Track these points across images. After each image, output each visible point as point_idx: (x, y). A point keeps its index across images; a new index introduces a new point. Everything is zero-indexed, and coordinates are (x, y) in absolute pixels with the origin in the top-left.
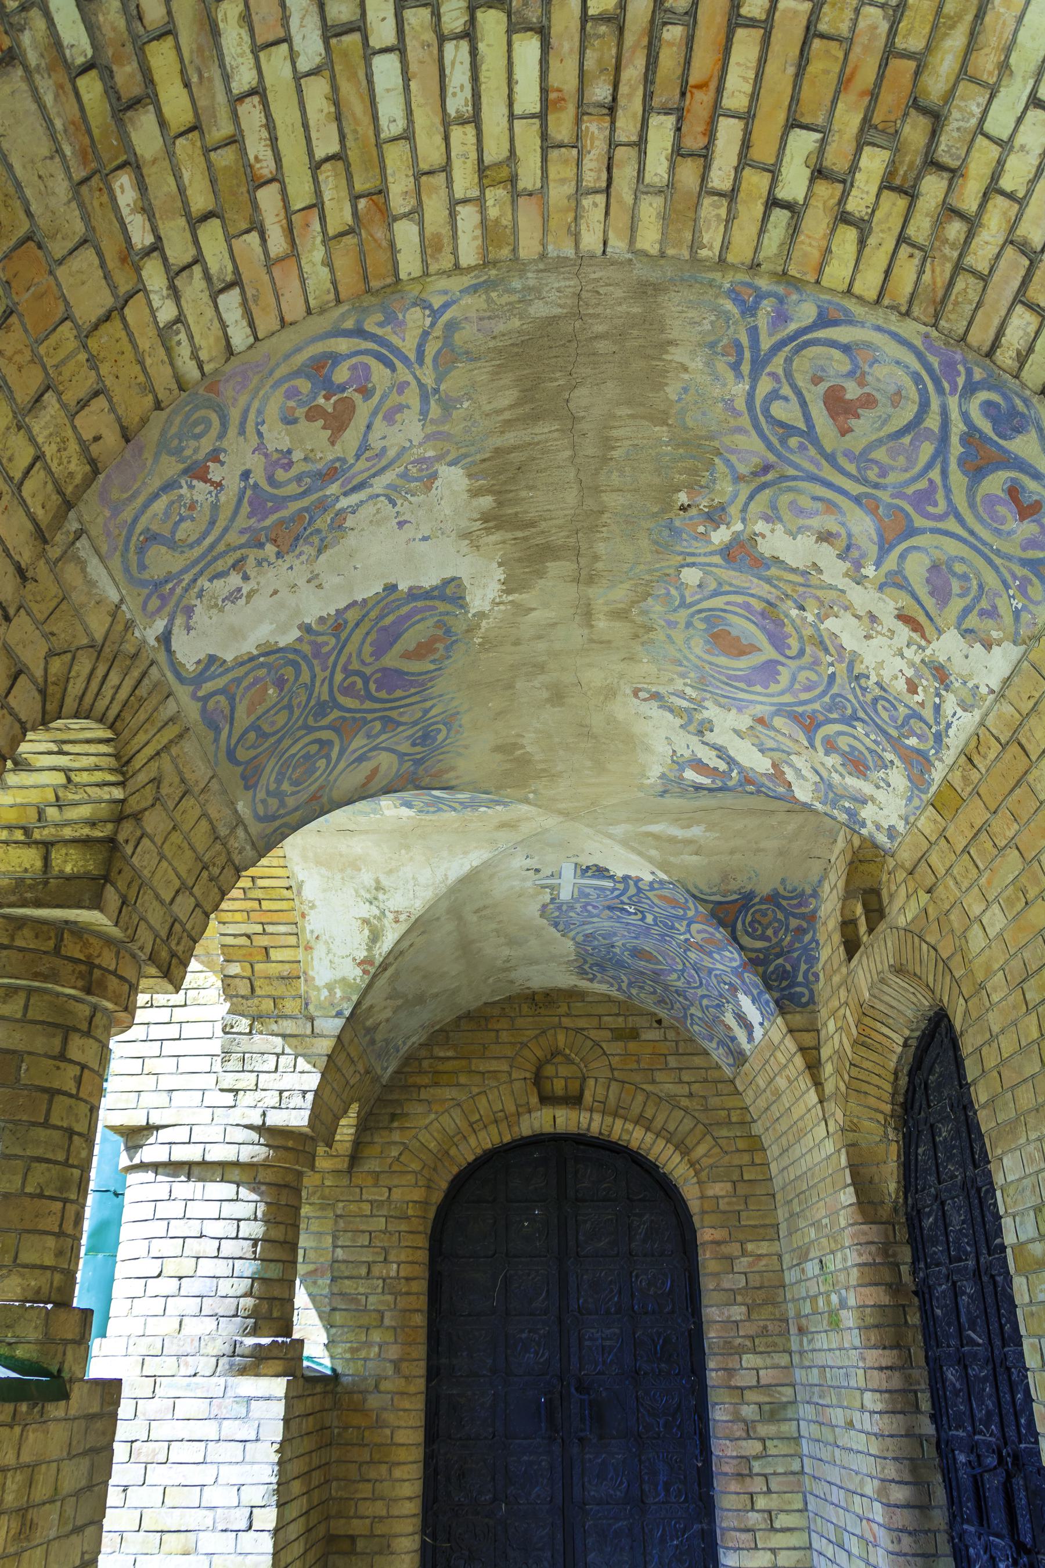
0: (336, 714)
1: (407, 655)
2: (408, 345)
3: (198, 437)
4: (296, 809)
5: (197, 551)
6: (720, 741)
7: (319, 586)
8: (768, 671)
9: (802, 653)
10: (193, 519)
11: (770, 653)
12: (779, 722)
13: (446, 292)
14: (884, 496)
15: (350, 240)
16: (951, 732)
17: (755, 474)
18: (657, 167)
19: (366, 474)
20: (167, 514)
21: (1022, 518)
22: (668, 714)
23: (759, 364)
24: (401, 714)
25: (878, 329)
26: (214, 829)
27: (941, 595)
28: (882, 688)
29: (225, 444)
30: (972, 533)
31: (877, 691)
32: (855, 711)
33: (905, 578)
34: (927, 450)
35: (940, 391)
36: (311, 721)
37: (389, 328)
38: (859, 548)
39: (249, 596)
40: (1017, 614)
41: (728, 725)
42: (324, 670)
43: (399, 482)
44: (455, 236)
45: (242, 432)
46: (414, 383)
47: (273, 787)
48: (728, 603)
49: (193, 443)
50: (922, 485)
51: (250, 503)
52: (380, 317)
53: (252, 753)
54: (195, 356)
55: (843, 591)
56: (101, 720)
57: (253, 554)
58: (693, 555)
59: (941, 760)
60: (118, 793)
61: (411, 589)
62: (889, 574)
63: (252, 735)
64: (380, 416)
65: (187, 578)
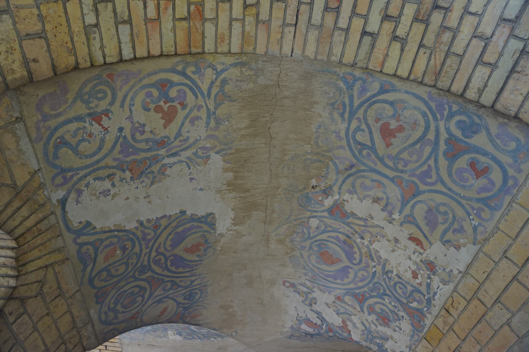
0: (150, 274)
1: (186, 250)
2: (204, 88)
3: (99, 99)
4: (123, 322)
5: (89, 161)
6: (319, 310)
7: (150, 202)
8: (345, 271)
9: (361, 261)
10: (90, 143)
11: (346, 262)
12: (347, 299)
13: (223, 64)
14: (406, 176)
15: (185, 24)
16: (436, 297)
17: (346, 170)
18: (317, 17)
19: (178, 149)
20: (75, 135)
21: (478, 177)
22: (297, 295)
23: (352, 113)
24: (181, 281)
25: (407, 92)
26: (74, 321)
27: (432, 224)
28: (399, 277)
29: (112, 109)
30: (450, 189)
31: (397, 279)
32: (385, 291)
33: (414, 218)
34: (428, 150)
35: (435, 119)
36: (137, 274)
37: (197, 76)
38: (392, 204)
39: (114, 196)
40: (475, 228)
41: (323, 299)
42: (147, 248)
43: (193, 157)
44: (230, 37)
45: (122, 106)
46: (205, 106)
47: (112, 306)
48: (329, 237)
49: (96, 102)
50: (425, 168)
51: (121, 146)
52: (193, 69)
53: (103, 284)
54: (102, 48)
55: (383, 228)
56: (10, 233)
57: (119, 174)
58: (316, 212)
59: (430, 313)
60: (12, 282)
61: (192, 215)
62: (406, 216)
63: (105, 274)
64: (188, 120)
65: (82, 173)
